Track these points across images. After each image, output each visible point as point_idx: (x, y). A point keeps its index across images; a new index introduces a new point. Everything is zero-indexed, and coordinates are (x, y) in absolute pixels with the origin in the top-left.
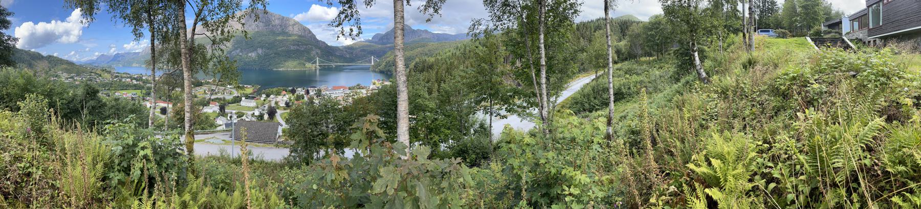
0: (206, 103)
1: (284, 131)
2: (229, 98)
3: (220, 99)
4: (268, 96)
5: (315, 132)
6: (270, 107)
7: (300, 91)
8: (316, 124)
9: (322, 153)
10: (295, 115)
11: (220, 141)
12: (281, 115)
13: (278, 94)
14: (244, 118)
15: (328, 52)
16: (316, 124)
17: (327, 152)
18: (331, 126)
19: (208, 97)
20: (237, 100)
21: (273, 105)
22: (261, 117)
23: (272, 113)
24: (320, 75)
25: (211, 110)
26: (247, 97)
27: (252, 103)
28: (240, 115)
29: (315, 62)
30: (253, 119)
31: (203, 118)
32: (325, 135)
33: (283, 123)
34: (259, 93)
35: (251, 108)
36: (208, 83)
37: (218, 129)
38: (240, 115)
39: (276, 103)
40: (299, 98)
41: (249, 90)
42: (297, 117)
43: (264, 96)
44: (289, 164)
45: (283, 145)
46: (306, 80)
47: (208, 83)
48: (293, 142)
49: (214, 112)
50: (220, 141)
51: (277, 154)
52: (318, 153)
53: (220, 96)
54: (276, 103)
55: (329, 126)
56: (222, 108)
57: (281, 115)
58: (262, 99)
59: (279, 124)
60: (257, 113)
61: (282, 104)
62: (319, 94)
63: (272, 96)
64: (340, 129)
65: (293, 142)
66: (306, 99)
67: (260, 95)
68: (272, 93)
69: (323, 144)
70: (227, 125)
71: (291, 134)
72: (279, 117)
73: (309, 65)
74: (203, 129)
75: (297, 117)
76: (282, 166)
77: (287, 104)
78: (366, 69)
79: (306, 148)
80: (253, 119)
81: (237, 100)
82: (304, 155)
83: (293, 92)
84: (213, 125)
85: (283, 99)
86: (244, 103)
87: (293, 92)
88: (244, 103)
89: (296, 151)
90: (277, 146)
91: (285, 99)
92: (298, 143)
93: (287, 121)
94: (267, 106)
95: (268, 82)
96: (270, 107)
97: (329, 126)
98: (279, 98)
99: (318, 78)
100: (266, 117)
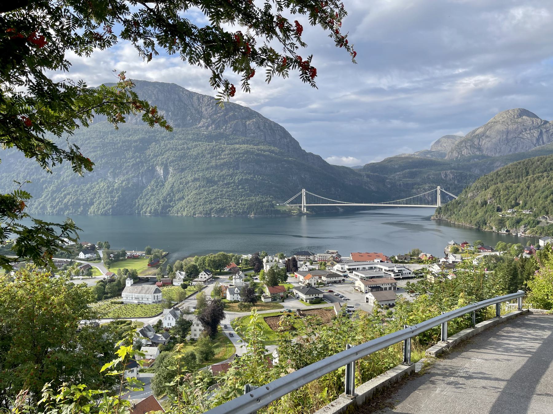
26: (138, 281)
98: (224, 281)
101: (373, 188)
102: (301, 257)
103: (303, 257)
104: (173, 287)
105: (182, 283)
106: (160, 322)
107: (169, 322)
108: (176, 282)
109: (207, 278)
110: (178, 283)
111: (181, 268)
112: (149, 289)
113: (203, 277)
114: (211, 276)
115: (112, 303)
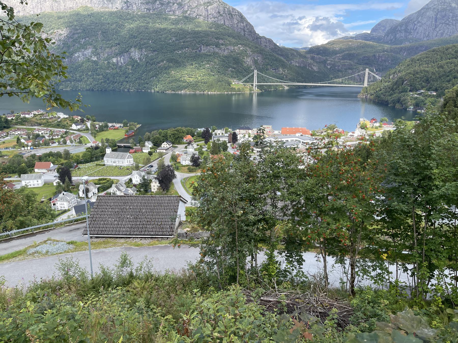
0: (25, 167)
1: (189, 213)
2: (77, 150)
3: (58, 155)
4: (157, 144)
5: (248, 216)
6: (162, 167)
7: (220, 135)
8: (252, 200)
9: (262, 257)
10: (212, 181)
11: (62, 246)
12: (184, 182)
13: (176, 140)
14: (111, 190)
15: (273, 57)
16: (252, 200)
17: (271, 257)
18: (280, 204)
19: (28, 151)
20: (95, 155)
21: (167, 162)
22: (145, 186)
23: (166, 178)
24: (261, 104)
25: (39, 180)
26: (116, 148)
27: (127, 160)
28: (104, 185)
29: (250, 80)
30: (131, 191)
31: (19, 200)
32: (270, 223)
33: (188, 197)
34: (138, 139)
35: (124, 169)
36: (24, 121)
37: (59, 220)
38: (104, 185)
39: (174, 158)
40: (219, 148)
41: (117, 132)
42: (217, 184)
43: (149, 145)
44: (201, 282)
45: (189, 239)
46: (232, 114)
47: (24, 121)
48: (206, 235)
49: (47, 184)
50: (62, 246)
51: (175, 260)
52: (254, 258)
53: (55, 148)
54: (174, 158)
55: (277, 204)
56: (65, 174)
57: (184, 182)
58: (146, 151)
59: (180, 199)
60: (137, 180)
61: (186, 161)
62: (259, 141)
63: (165, 145)
64: (297, 212)
65: (206, 235)
66: (231, 151)
67: (141, 143)
68: (165, 139)
69: (263, 240)
70: (79, 209)
71: (204, 218)
72: (179, 186)
73: (236, 84)
74: (22, 225)
75: (217, 184)
76: (184, 284)
77: (195, 161)
78: (350, 96)
79: (232, 247)
80: (131, 191)
81: (95, 155)
82: (229, 260)
83: (206, 136)
84: (46, 214)
85: (185, 153)
86: (111, 159)
87: (206, 136)
88: (111, 159)
89: (213, 252)
90: (176, 243)
91: (191, 150)
92: (218, 236)
93: (196, 192)
94: (155, 165)
95: (157, 121)
96: (162, 167)
97: (277, 204)
99: (255, 112)
100: (155, 186)
101: (315, 68)
102: (242, 131)
103: (244, 131)
104: (143, 153)
105: (150, 150)
106: (131, 180)
107: (137, 180)
108: (144, 149)
109: (168, 147)
110: (146, 151)
111: (148, 139)
112: (123, 155)
113: (165, 146)
114: (171, 145)
115: (97, 165)
